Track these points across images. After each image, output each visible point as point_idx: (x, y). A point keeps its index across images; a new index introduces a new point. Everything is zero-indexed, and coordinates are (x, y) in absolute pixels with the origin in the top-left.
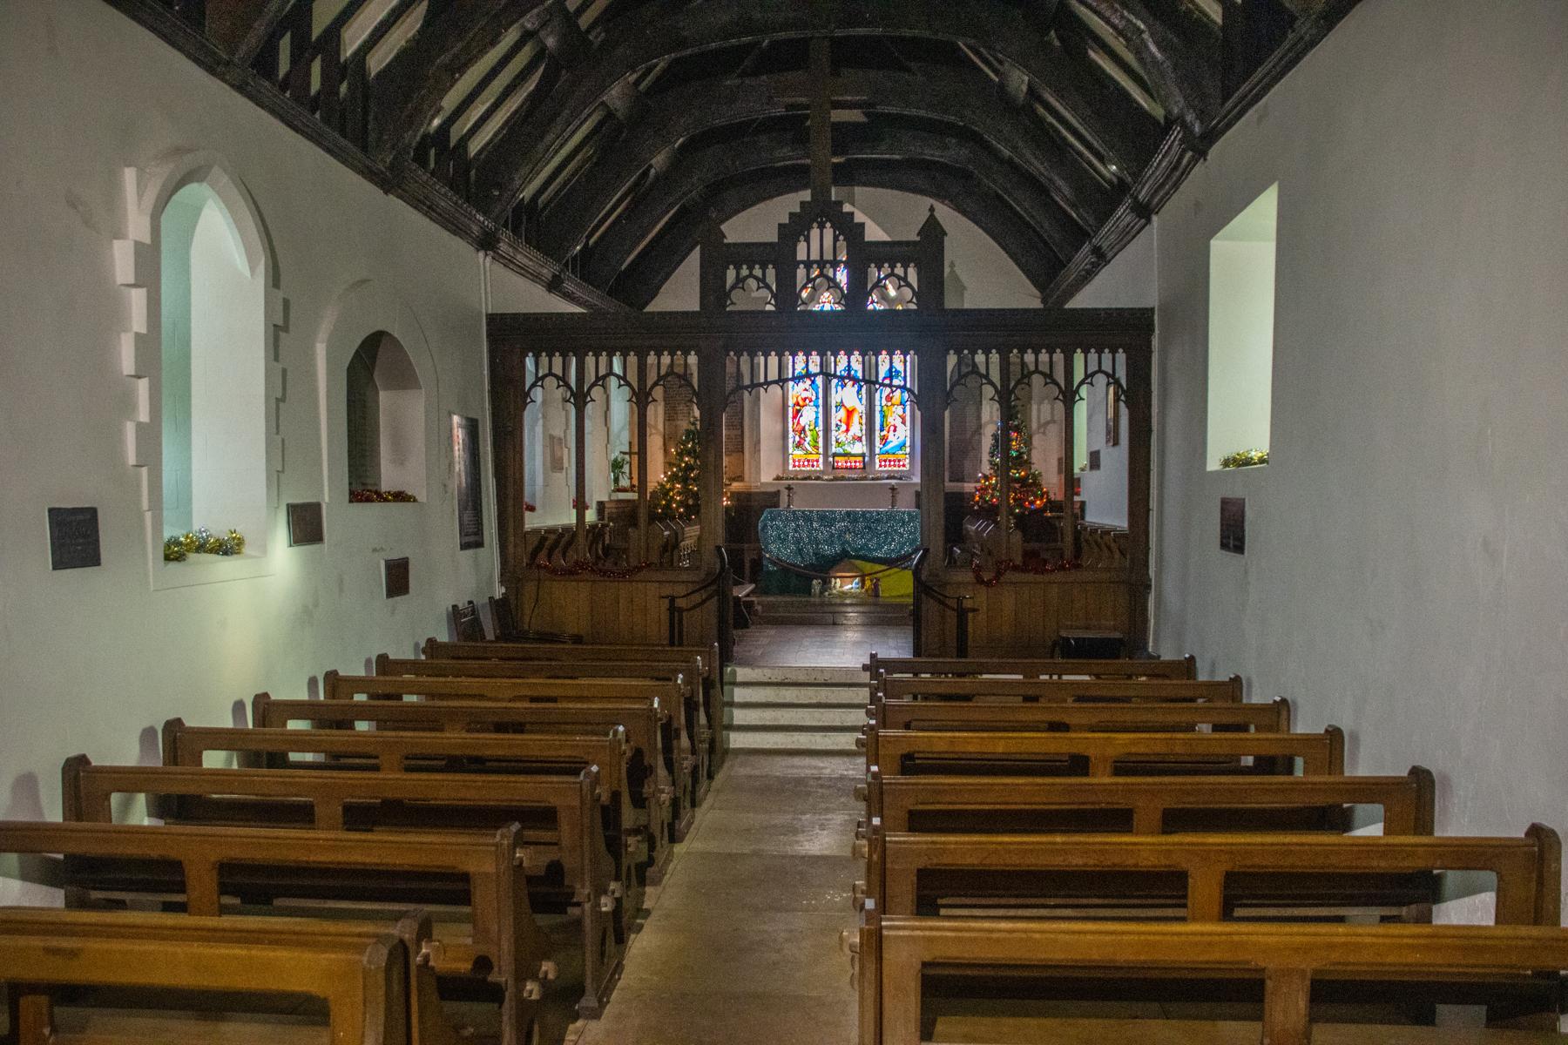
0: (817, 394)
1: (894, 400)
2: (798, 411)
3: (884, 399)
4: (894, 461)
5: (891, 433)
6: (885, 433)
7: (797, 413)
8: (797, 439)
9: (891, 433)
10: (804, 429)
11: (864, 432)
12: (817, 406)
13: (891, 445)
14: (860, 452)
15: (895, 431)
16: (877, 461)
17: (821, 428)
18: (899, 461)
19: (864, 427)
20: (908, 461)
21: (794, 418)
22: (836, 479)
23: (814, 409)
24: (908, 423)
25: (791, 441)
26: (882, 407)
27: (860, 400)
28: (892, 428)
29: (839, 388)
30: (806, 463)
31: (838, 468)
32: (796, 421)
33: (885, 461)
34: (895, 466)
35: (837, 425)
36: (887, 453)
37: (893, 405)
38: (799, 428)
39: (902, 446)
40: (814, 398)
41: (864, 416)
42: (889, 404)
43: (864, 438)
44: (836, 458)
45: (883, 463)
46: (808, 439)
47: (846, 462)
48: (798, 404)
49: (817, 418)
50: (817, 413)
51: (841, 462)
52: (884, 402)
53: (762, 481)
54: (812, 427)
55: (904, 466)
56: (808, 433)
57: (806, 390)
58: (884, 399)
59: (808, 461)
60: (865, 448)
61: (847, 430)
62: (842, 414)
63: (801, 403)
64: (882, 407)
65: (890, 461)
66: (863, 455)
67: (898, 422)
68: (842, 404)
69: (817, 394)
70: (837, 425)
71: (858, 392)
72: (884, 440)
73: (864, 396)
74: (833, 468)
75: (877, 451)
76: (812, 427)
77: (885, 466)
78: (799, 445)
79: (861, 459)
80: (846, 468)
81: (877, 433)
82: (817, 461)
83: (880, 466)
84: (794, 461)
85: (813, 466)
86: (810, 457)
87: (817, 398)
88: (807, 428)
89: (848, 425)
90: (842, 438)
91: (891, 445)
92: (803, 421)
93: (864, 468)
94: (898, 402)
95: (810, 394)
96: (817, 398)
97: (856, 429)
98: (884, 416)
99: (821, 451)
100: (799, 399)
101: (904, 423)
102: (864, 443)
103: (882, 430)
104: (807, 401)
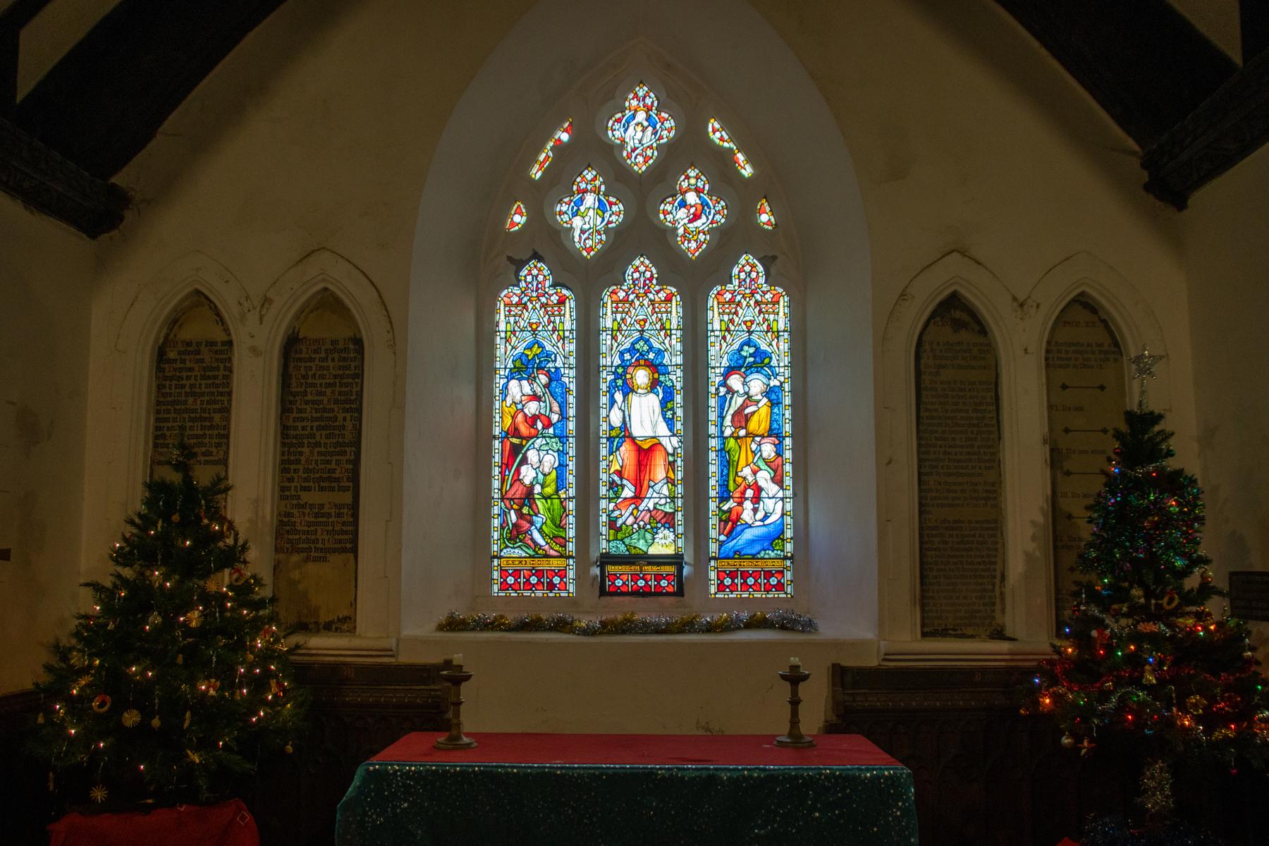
0: (563, 407)
1: (753, 425)
2: (516, 450)
3: (729, 418)
4: (756, 575)
5: (748, 505)
6: (731, 504)
7: (515, 455)
9: (748, 505)
10: (529, 494)
11: (680, 502)
12: (562, 438)
13: (748, 535)
14: (670, 551)
15: (757, 499)
16: (713, 575)
17: (572, 492)
18: (769, 574)
20: (788, 575)
21: (506, 465)
22: (609, 628)
23: (556, 445)
24: (788, 481)
26: (721, 436)
27: (670, 423)
28: (749, 493)
29: (619, 397)
30: (534, 580)
31: (616, 593)
33: (732, 575)
34: (756, 586)
35: (612, 485)
36: (738, 554)
38: (518, 491)
39: (775, 538)
40: (555, 418)
42: (742, 433)
44: (611, 569)
45: (728, 581)
47: (635, 578)
48: (515, 431)
49: (562, 466)
50: (562, 453)
51: (622, 577)
53: (407, 632)
54: (549, 490)
55: (780, 587)
56: (540, 504)
57: (535, 397)
58: (729, 418)
59: (539, 574)
60: (680, 543)
61: (638, 497)
62: (626, 454)
63: (524, 429)
65: (745, 575)
66: (676, 559)
67: (764, 478)
68: (625, 433)
69: (563, 407)
70: (612, 485)
71: (665, 403)
72: (731, 523)
73: (680, 412)
74: (603, 592)
75: (713, 548)
76: (549, 490)
77: (733, 588)
78: (516, 535)
79: (671, 569)
80: (636, 593)
81: (713, 506)
82: (562, 574)
83: (721, 588)
84: (504, 573)
85: (551, 586)
86: (544, 565)
87: (563, 417)
88: (538, 489)
89: (638, 484)
90: (626, 517)
91: (748, 535)
92: (527, 474)
93: (680, 592)
94: (764, 427)
96: (563, 417)
97: (658, 495)
98: (728, 463)
99: (571, 547)
100: (520, 417)
101: (778, 480)
102: (680, 530)
103: (724, 498)
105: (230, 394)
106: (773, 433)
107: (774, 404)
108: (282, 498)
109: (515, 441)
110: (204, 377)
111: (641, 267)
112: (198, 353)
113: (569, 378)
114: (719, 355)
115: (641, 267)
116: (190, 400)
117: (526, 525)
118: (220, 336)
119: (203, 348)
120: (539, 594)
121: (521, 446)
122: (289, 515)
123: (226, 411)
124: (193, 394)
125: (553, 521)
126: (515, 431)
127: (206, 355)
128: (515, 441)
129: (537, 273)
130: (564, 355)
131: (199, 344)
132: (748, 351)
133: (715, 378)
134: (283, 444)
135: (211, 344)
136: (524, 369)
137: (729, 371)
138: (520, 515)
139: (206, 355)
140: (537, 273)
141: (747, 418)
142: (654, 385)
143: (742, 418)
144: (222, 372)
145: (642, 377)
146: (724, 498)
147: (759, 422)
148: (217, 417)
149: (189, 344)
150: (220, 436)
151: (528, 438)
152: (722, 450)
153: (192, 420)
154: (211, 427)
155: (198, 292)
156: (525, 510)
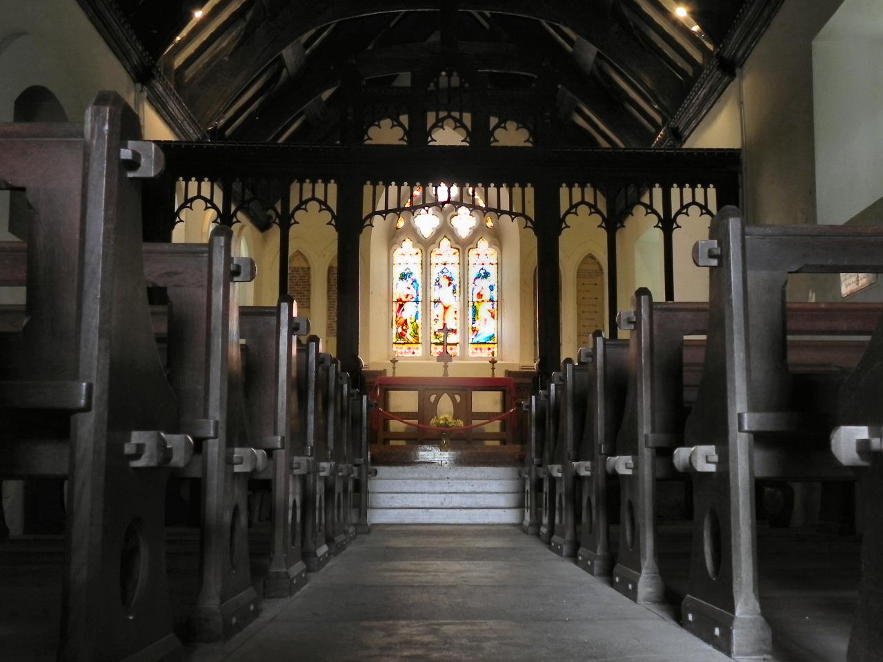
1: (484, 298)
2: (401, 306)
8: (400, 330)
10: (405, 322)
12: (417, 302)
19: (458, 321)
25: (394, 331)
26: (473, 302)
32: (399, 315)
37: (483, 301)
38: (401, 321)
40: (415, 296)
41: (458, 312)
42: (480, 300)
43: (458, 332)
46: (410, 330)
52: (475, 299)
63: (404, 299)
64: (473, 302)
71: (454, 291)
76: (413, 320)
77: (477, 353)
85: (413, 353)
95: (413, 292)
104: (409, 298)
105: (310, 285)
106: (491, 300)
107: (492, 290)
108: (329, 319)
109: (401, 303)
110: (301, 279)
111: (445, 243)
112: (298, 271)
113: (419, 281)
114: (473, 273)
115: (445, 243)
116: (296, 287)
117: (404, 333)
118: (304, 265)
119: (300, 270)
120: (409, 355)
121: (402, 305)
122: (330, 324)
123: (309, 291)
124: (297, 285)
125: (414, 331)
126: (399, 300)
127: (301, 272)
128: (401, 303)
129: (408, 245)
130: (417, 274)
131: (298, 268)
132: (482, 272)
133: (471, 281)
134: (329, 302)
135: (303, 268)
136: (403, 277)
137: (476, 278)
138: (403, 330)
139: (301, 272)
140: (408, 245)
141: (482, 295)
142: (450, 284)
143: (480, 295)
144: (307, 278)
145: (444, 282)
146: (473, 323)
147: (487, 296)
148: (306, 293)
149: (295, 268)
150: (307, 299)
151: (405, 302)
152: (474, 306)
153: (297, 293)
154: (304, 296)
155: (298, 251)
156: (404, 328)
